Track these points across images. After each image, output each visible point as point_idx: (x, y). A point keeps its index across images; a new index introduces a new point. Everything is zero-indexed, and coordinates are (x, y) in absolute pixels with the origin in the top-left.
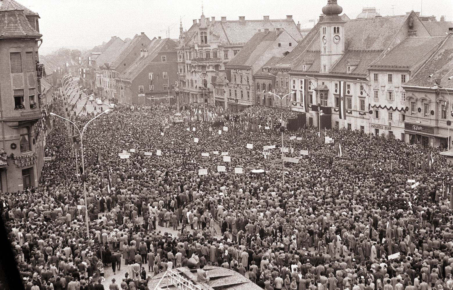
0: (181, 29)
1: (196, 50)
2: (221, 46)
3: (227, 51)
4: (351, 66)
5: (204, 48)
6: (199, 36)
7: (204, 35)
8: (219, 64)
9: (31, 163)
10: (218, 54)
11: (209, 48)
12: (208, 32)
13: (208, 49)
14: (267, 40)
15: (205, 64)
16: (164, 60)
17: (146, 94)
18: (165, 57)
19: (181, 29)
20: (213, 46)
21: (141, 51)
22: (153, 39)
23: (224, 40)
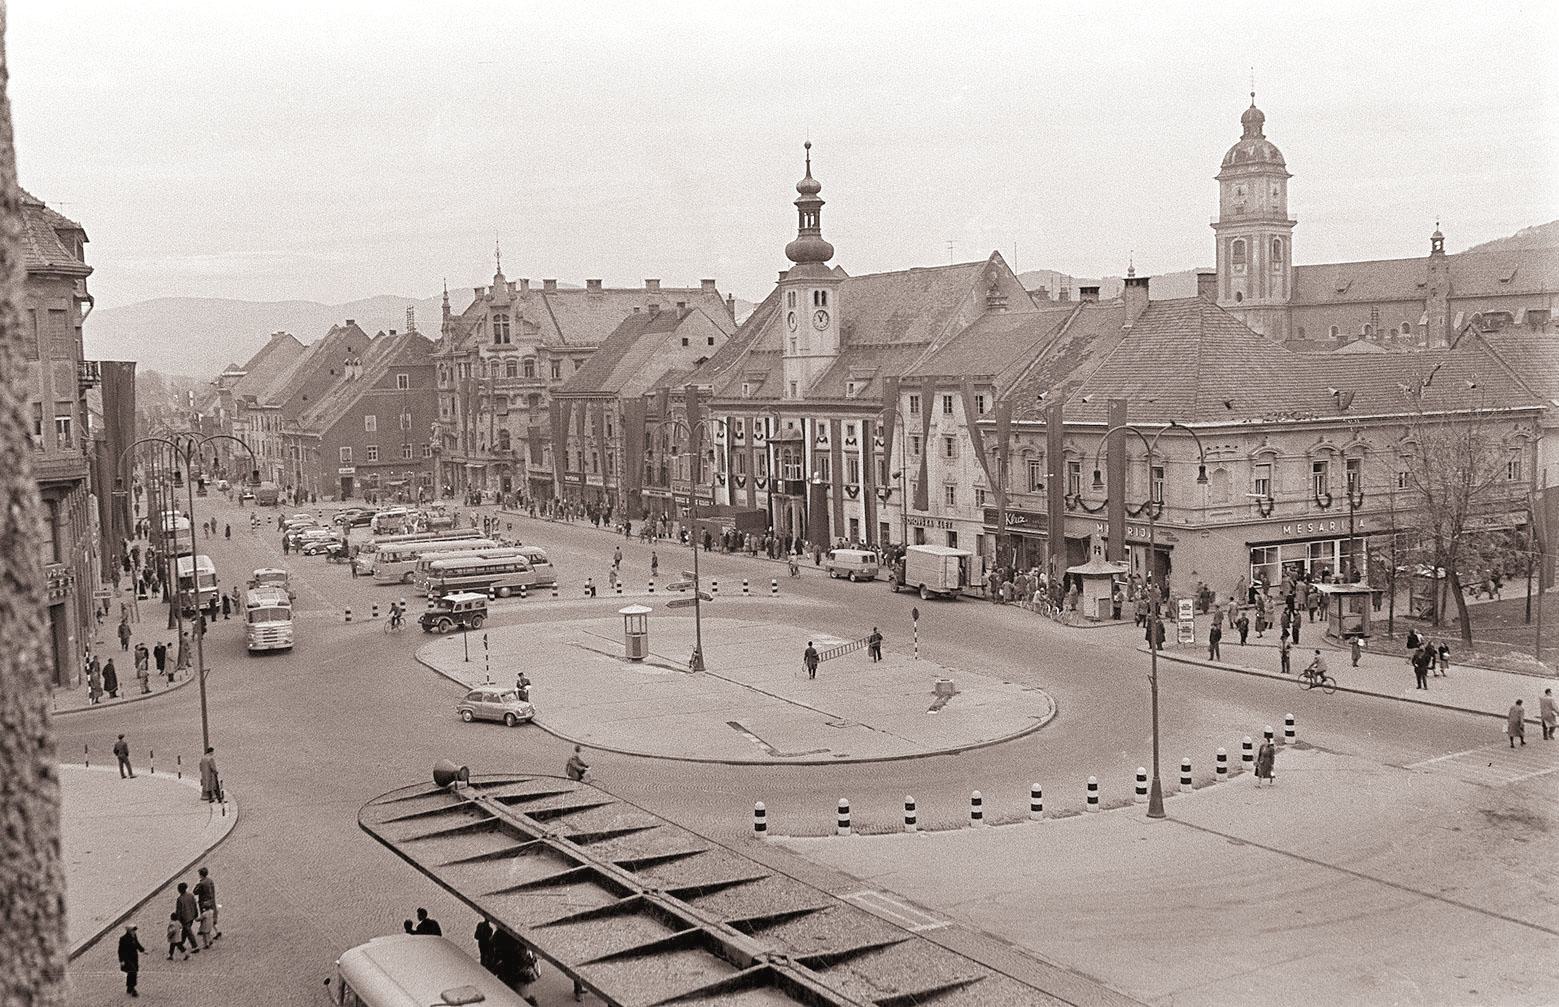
0: (446, 308)
1: (482, 358)
2: (544, 349)
3: (558, 361)
4: (857, 380)
5: (502, 354)
6: (490, 323)
7: (501, 322)
8: (539, 391)
9: (58, 593)
10: (537, 369)
12: (512, 315)
15: (505, 392)
16: (403, 384)
17: (358, 467)
18: (405, 377)
19: (446, 308)
20: (526, 350)
21: (347, 364)
22: (377, 336)
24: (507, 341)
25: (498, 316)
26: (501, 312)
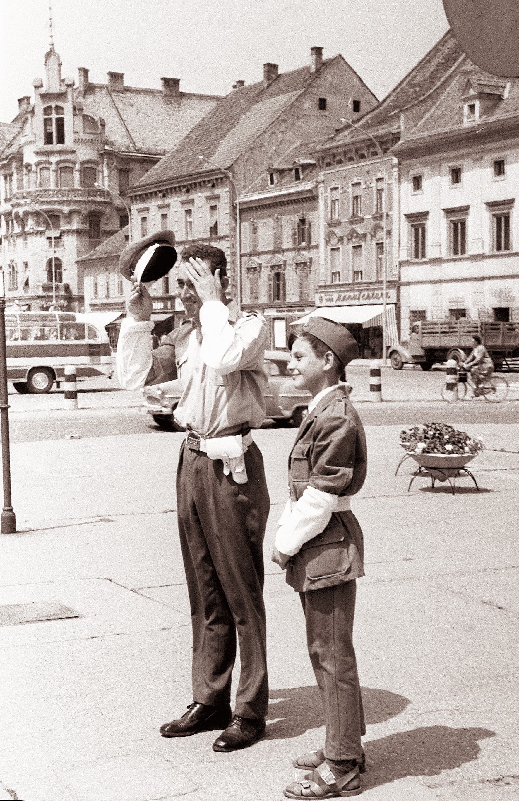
1: (28, 166)
6: (39, 117)
8: (102, 208)
11: (70, 157)
12: (68, 107)
13: (67, 161)
14: (273, 95)
23: (118, 137)
24: (61, 140)
25: (50, 107)
26: (53, 104)
